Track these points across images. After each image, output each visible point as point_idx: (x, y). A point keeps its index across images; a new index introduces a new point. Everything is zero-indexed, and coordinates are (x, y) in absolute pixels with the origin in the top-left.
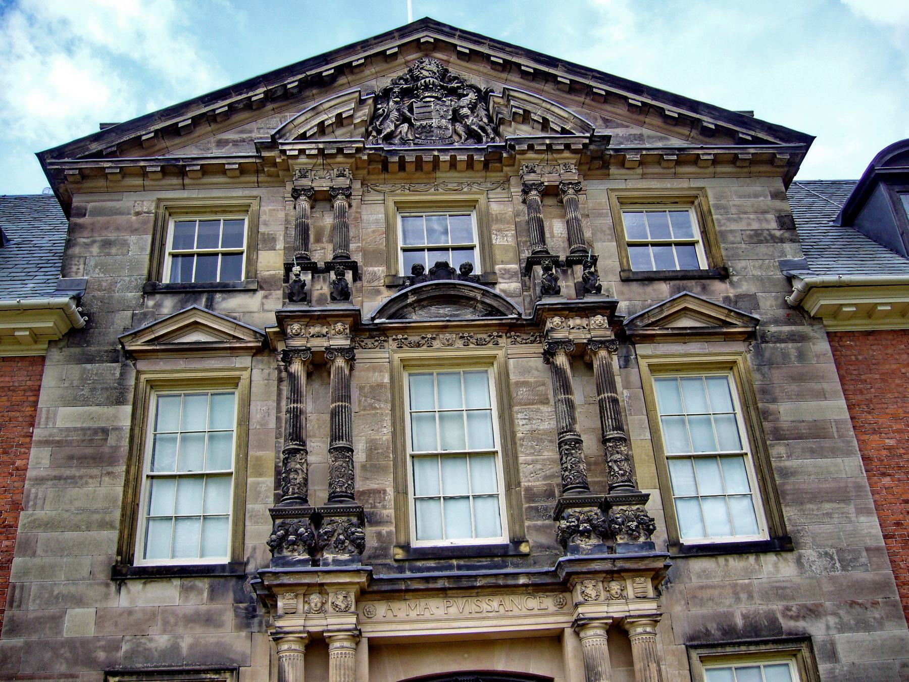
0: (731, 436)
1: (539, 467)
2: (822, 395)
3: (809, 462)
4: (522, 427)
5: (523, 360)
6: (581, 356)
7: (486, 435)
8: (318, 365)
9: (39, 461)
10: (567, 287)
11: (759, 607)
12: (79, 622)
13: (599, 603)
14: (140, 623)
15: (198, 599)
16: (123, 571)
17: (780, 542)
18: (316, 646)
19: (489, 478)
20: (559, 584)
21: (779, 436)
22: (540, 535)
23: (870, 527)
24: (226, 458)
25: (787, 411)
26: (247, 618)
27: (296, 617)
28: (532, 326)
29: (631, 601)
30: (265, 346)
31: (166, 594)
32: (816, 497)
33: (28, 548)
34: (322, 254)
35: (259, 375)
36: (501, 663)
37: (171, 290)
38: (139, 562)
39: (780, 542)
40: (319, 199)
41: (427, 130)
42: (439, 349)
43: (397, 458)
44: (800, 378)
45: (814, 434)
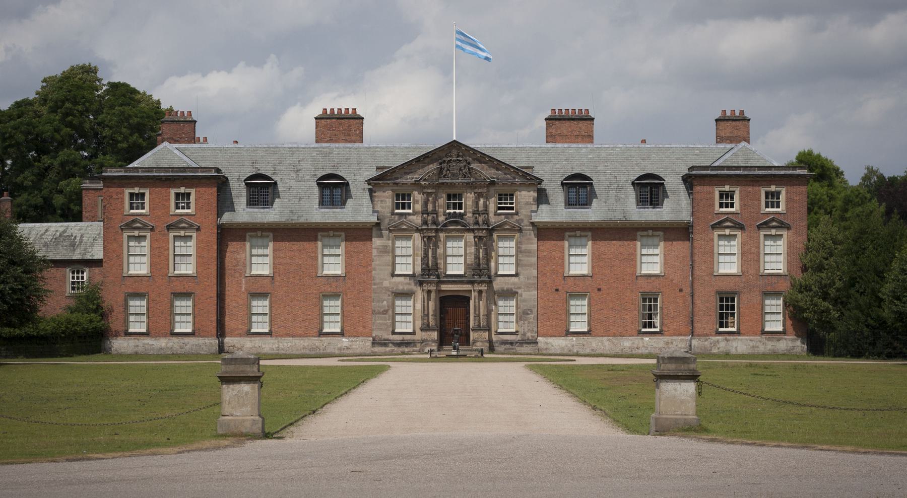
0: (513, 252)
1: (471, 259)
2: (532, 244)
3: (526, 258)
4: (468, 251)
5: (470, 237)
6: (480, 238)
7: (462, 252)
8: (429, 238)
9: (375, 252)
10: (480, 219)
11: (510, 286)
12: (386, 284)
13: (477, 287)
14: (398, 284)
15: (407, 280)
16: (393, 275)
17: (516, 275)
18: (429, 292)
19: (462, 260)
20: (472, 283)
21: (521, 252)
22: (469, 273)
23: (535, 272)
24: (410, 252)
25: (524, 247)
26: (416, 284)
27: (426, 287)
28: (473, 230)
29: (484, 287)
30: (417, 230)
31: (401, 279)
32: (526, 265)
33: (375, 269)
34: (430, 207)
35: (417, 236)
36: (461, 294)
37: (397, 214)
38: (396, 273)
39: (516, 275)
40: (429, 194)
41: (453, 174)
42: (453, 234)
43: (446, 256)
44: (529, 239)
45: (528, 253)
